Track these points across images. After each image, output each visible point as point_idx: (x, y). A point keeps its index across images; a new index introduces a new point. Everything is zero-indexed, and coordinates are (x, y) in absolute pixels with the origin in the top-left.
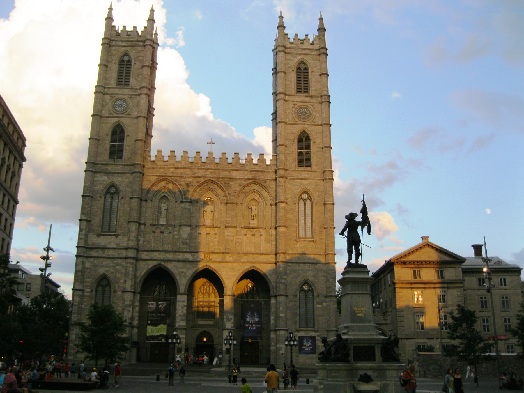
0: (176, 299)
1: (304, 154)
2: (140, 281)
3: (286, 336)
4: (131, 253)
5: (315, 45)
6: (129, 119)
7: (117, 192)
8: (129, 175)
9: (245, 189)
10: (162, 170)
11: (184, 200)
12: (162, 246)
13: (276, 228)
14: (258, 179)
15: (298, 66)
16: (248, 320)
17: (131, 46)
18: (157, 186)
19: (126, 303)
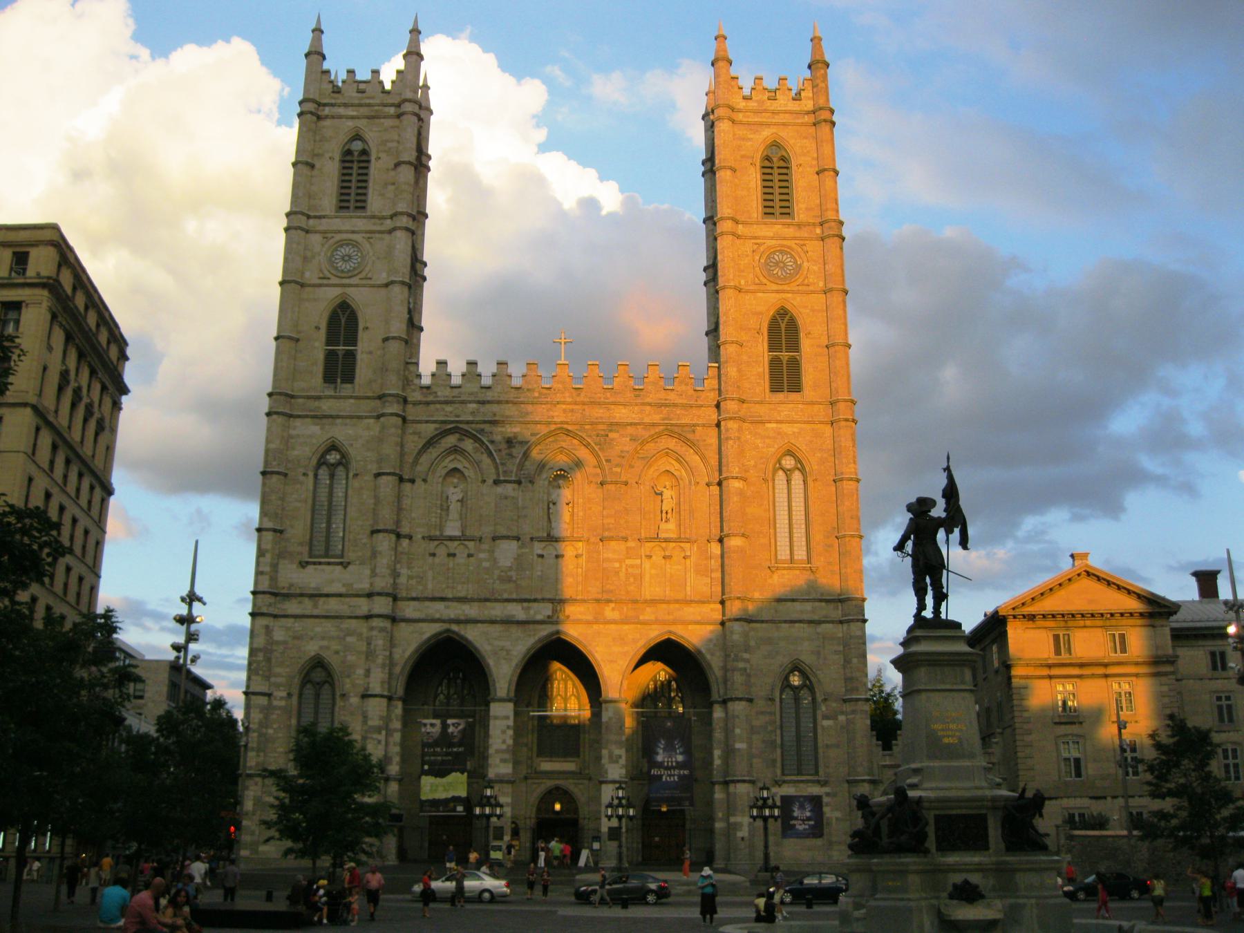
0: (489, 710)
1: (785, 362)
2: (403, 668)
3: (752, 795)
4: (381, 605)
5: (803, 102)
7: (344, 462)
8: (372, 421)
9: (645, 448)
10: (449, 408)
11: (502, 478)
12: (453, 588)
13: (721, 541)
14: (676, 425)
16: (659, 758)
18: (438, 446)
19: (370, 723)
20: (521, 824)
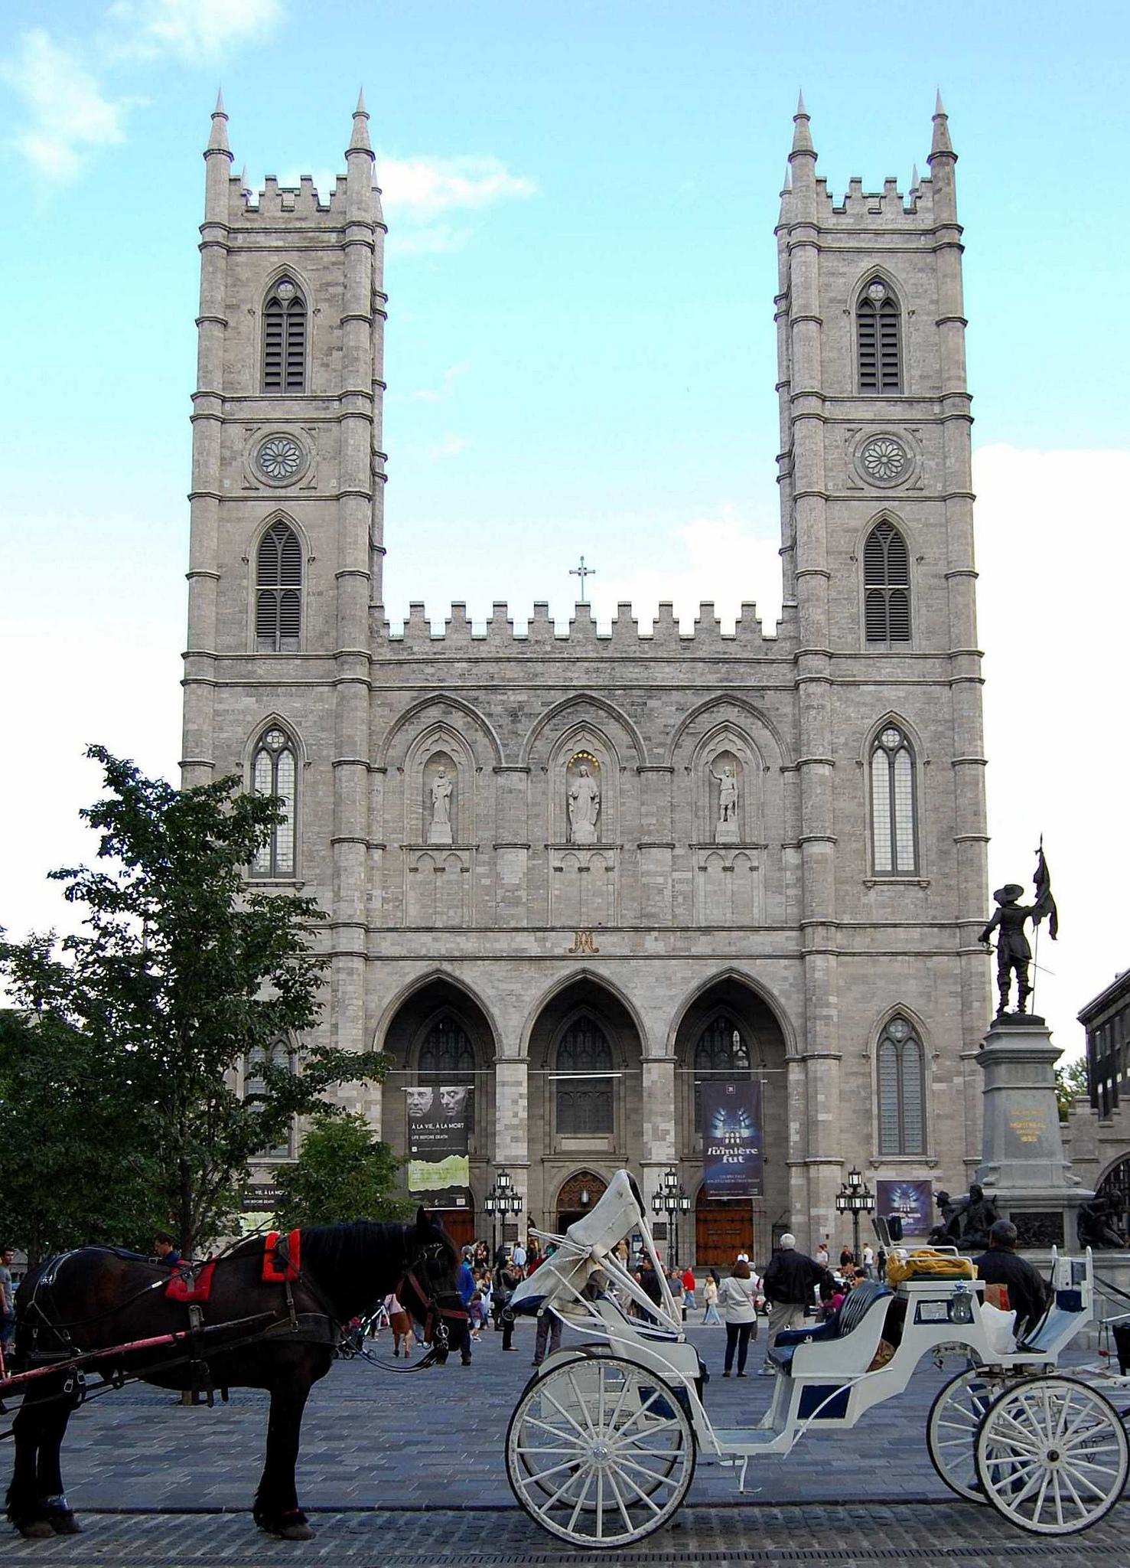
1: (887, 599)
7: (291, 746)
8: (327, 689)
10: (429, 670)
13: (799, 846)
14: (738, 688)
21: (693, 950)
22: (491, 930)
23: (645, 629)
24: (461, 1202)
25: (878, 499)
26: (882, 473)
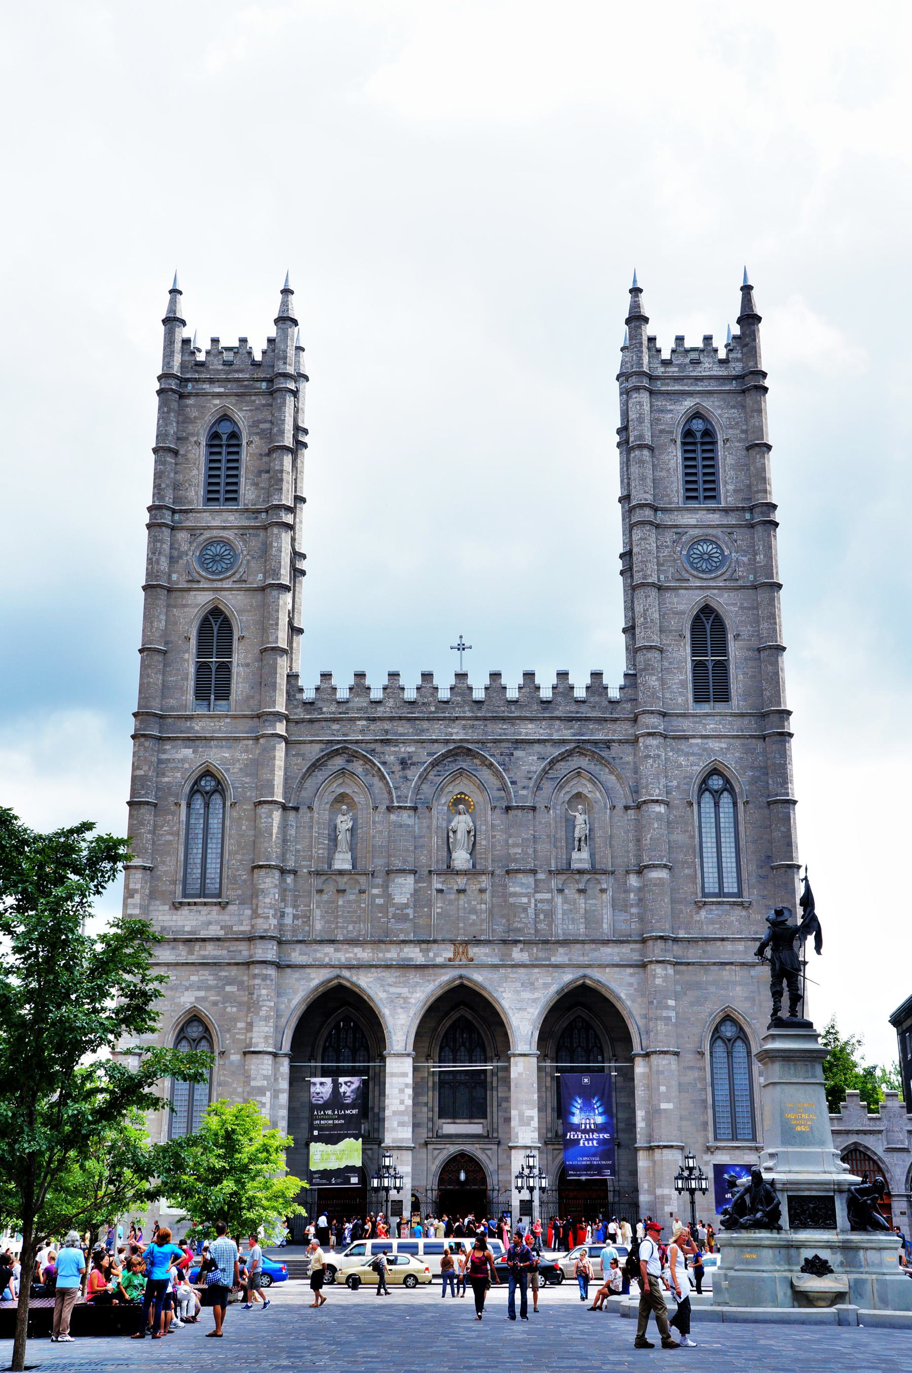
0: (385, 1066)
5: (732, 364)
6: (242, 593)
7: (220, 788)
8: (251, 742)
10: (335, 727)
11: (396, 804)
12: (343, 928)
13: (640, 871)
14: (588, 741)
15: (687, 427)
16: (576, 1120)
17: (237, 395)
18: (323, 768)
19: (253, 1083)
20: (422, 1198)
21: (553, 959)
22: (383, 942)
23: (512, 694)
24: (354, 1180)
25: (701, 588)
26: (704, 567)
